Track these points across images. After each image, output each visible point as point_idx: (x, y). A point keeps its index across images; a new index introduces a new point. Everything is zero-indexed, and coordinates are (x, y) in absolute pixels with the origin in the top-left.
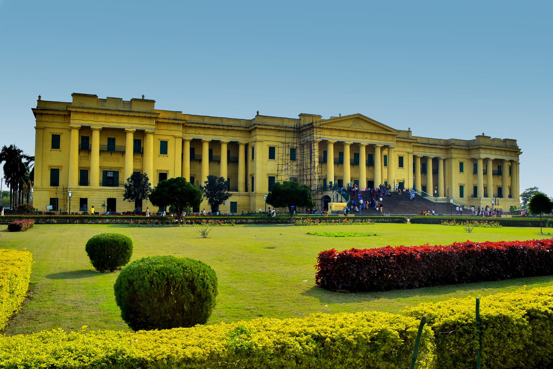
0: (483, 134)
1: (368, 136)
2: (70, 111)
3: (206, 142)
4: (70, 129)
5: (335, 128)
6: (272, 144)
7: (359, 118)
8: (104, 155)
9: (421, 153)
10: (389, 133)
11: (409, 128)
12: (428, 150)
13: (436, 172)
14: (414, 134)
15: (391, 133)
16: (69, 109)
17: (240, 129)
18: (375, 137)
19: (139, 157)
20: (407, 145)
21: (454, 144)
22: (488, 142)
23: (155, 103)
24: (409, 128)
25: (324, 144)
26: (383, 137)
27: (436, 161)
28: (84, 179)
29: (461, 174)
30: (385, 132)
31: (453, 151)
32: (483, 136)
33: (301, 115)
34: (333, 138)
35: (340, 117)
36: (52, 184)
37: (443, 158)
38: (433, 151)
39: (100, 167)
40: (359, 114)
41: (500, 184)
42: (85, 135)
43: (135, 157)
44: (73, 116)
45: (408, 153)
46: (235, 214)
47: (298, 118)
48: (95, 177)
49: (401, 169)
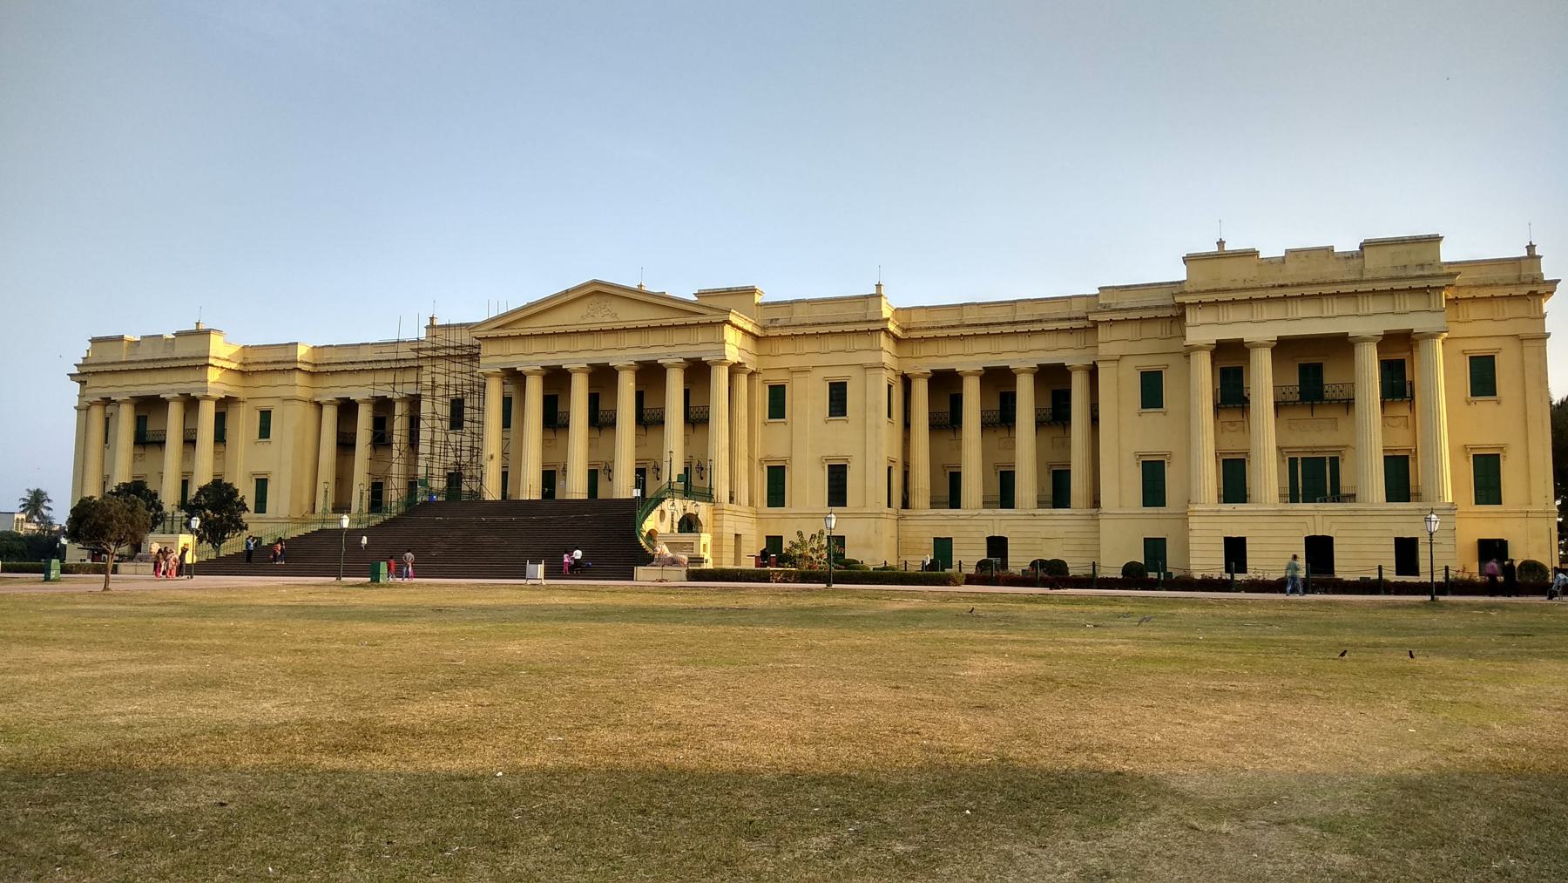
0: (1221, 243)
2: (1182, 306)
3: (1023, 371)
4: (1188, 352)
5: (528, 332)
7: (598, 292)
8: (1224, 416)
9: (969, 360)
11: (879, 286)
16: (1178, 299)
17: (1074, 324)
19: (1403, 410)
21: (1106, 308)
22: (1231, 274)
23: (1442, 245)
24: (879, 286)
25: (515, 377)
26: (678, 337)
27: (1053, 379)
28: (1235, 484)
29: (1152, 415)
30: (681, 321)
31: (1102, 333)
32: (1222, 255)
35: (639, 291)
36: (1147, 502)
39: (1279, 449)
40: (595, 282)
41: (1401, 441)
42: (1231, 364)
43: (1390, 412)
44: (1191, 317)
46: (1239, 577)
48: (1267, 476)
49: (838, 423)
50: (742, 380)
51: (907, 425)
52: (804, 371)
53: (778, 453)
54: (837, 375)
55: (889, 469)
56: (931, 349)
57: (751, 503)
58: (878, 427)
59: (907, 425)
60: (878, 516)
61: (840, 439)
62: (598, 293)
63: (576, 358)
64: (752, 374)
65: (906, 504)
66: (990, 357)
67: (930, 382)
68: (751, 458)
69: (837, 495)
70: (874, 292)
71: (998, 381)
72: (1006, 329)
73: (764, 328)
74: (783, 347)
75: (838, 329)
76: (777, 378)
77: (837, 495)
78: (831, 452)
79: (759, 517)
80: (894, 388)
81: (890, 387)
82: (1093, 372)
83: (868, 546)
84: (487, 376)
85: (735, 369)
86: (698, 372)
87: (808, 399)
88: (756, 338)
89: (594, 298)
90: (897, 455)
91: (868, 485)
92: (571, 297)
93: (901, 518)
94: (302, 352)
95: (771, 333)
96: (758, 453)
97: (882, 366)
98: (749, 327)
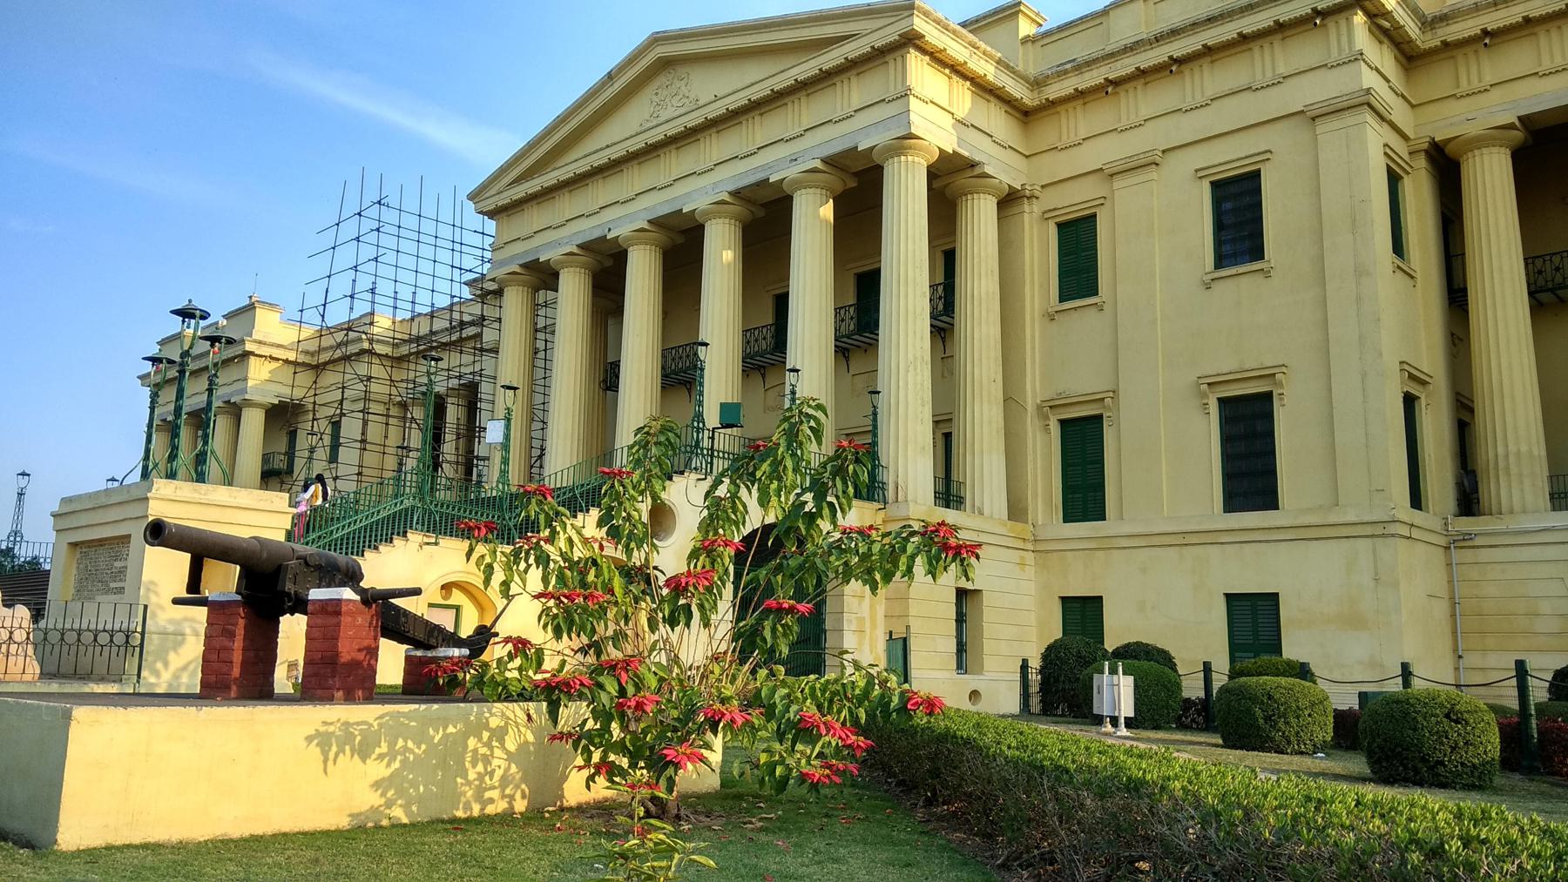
7: (663, 60)
15: (852, 50)
50: (980, 216)
51: (1457, 297)
53: (1081, 381)
54: (1229, 157)
55: (1410, 401)
56: (1517, 58)
57: (1016, 511)
58: (1361, 272)
59: (1457, 297)
60: (1380, 530)
61: (1248, 328)
64: (1009, 201)
65: (1469, 501)
67: (1521, 159)
68: (1011, 401)
69: (1250, 474)
73: (1037, 84)
74: (1080, 122)
75: (1227, 31)
77: (1250, 474)
78: (1224, 362)
79: (1040, 548)
80: (1408, 186)
81: (1394, 179)
83: (1353, 620)
85: (949, 182)
86: (859, 190)
88: (1025, 115)
89: (662, 79)
90: (1432, 359)
91: (1343, 443)
92: (618, 85)
93: (1456, 543)
94: (383, 323)
95: (1055, 91)
96: (1034, 390)
97: (1365, 102)
98: (987, 69)
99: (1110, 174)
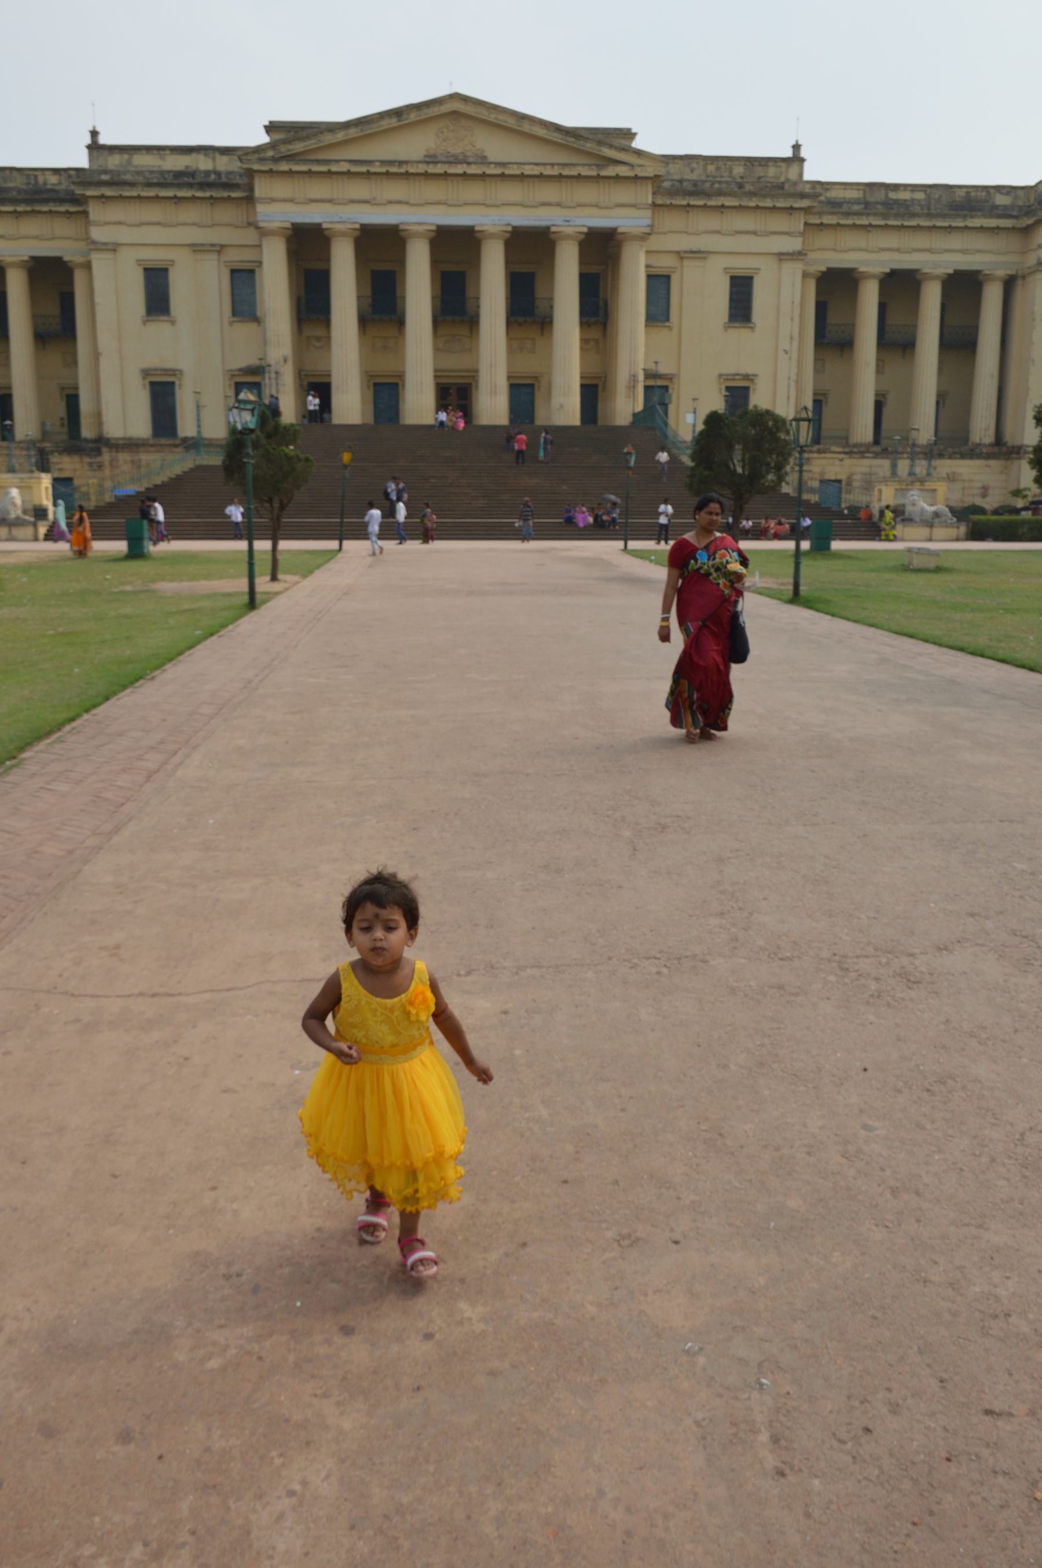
1: (512, 192)
5: (344, 167)
6: (155, 256)
7: (457, 112)
10: (610, 171)
11: (796, 147)
12: (921, 241)
13: (959, 343)
14: (811, 173)
15: (622, 171)
18: (549, 192)
20: (779, 223)
24: (796, 147)
27: (963, 288)
33: (271, 128)
34: (343, 210)
37: (1001, 273)
38: (955, 241)
40: (456, 97)
45: (782, 257)
47: (264, 139)
52: (699, 255)
54: (742, 265)
62: (455, 114)
63: (419, 212)
66: (897, 256)
70: (788, 153)
71: (900, 285)
72: (924, 223)
76: (663, 263)
82: (1009, 284)
84: (263, 233)
87: (702, 295)
99: (681, 255)
